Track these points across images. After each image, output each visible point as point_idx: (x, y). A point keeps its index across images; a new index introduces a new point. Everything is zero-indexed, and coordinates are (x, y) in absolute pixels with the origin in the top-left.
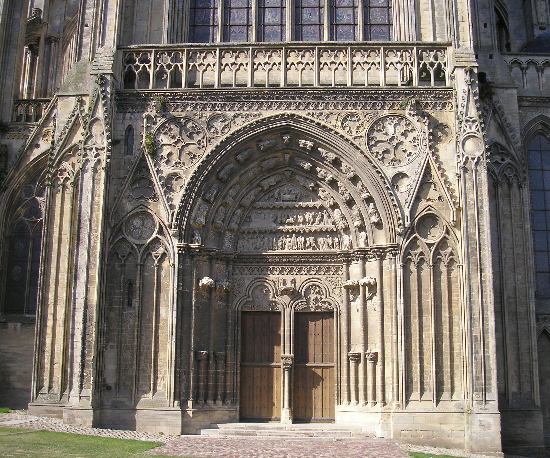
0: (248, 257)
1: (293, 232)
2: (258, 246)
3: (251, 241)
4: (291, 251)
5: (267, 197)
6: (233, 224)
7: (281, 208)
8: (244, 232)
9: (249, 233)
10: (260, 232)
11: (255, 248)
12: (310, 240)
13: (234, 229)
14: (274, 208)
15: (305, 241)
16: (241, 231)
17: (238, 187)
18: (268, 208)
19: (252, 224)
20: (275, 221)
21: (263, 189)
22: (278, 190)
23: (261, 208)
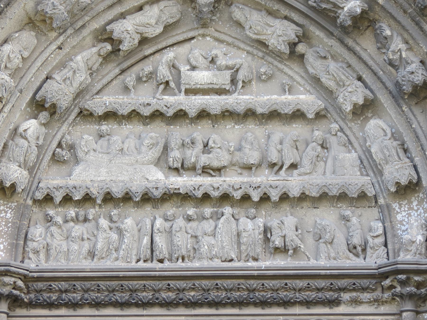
0: (64, 285)
1: (225, 198)
2: (99, 246)
3: (78, 230)
4: (217, 263)
5: (130, 78)
6: (14, 167)
7: (180, 115)
8: (48, 199)
9: (67, 199)
10: (108, 198)
11: (92, 254)
12: (286, 223)
13: (13, 186)
14: (157, 115)
15: (267, 230)
16: (39, 196)
17: (28, 37)
18: (134, 115)
19: (78, 169)
20: (161, 161)
21: (116, 51)
22: (170, 55)
23: (110, 115)
